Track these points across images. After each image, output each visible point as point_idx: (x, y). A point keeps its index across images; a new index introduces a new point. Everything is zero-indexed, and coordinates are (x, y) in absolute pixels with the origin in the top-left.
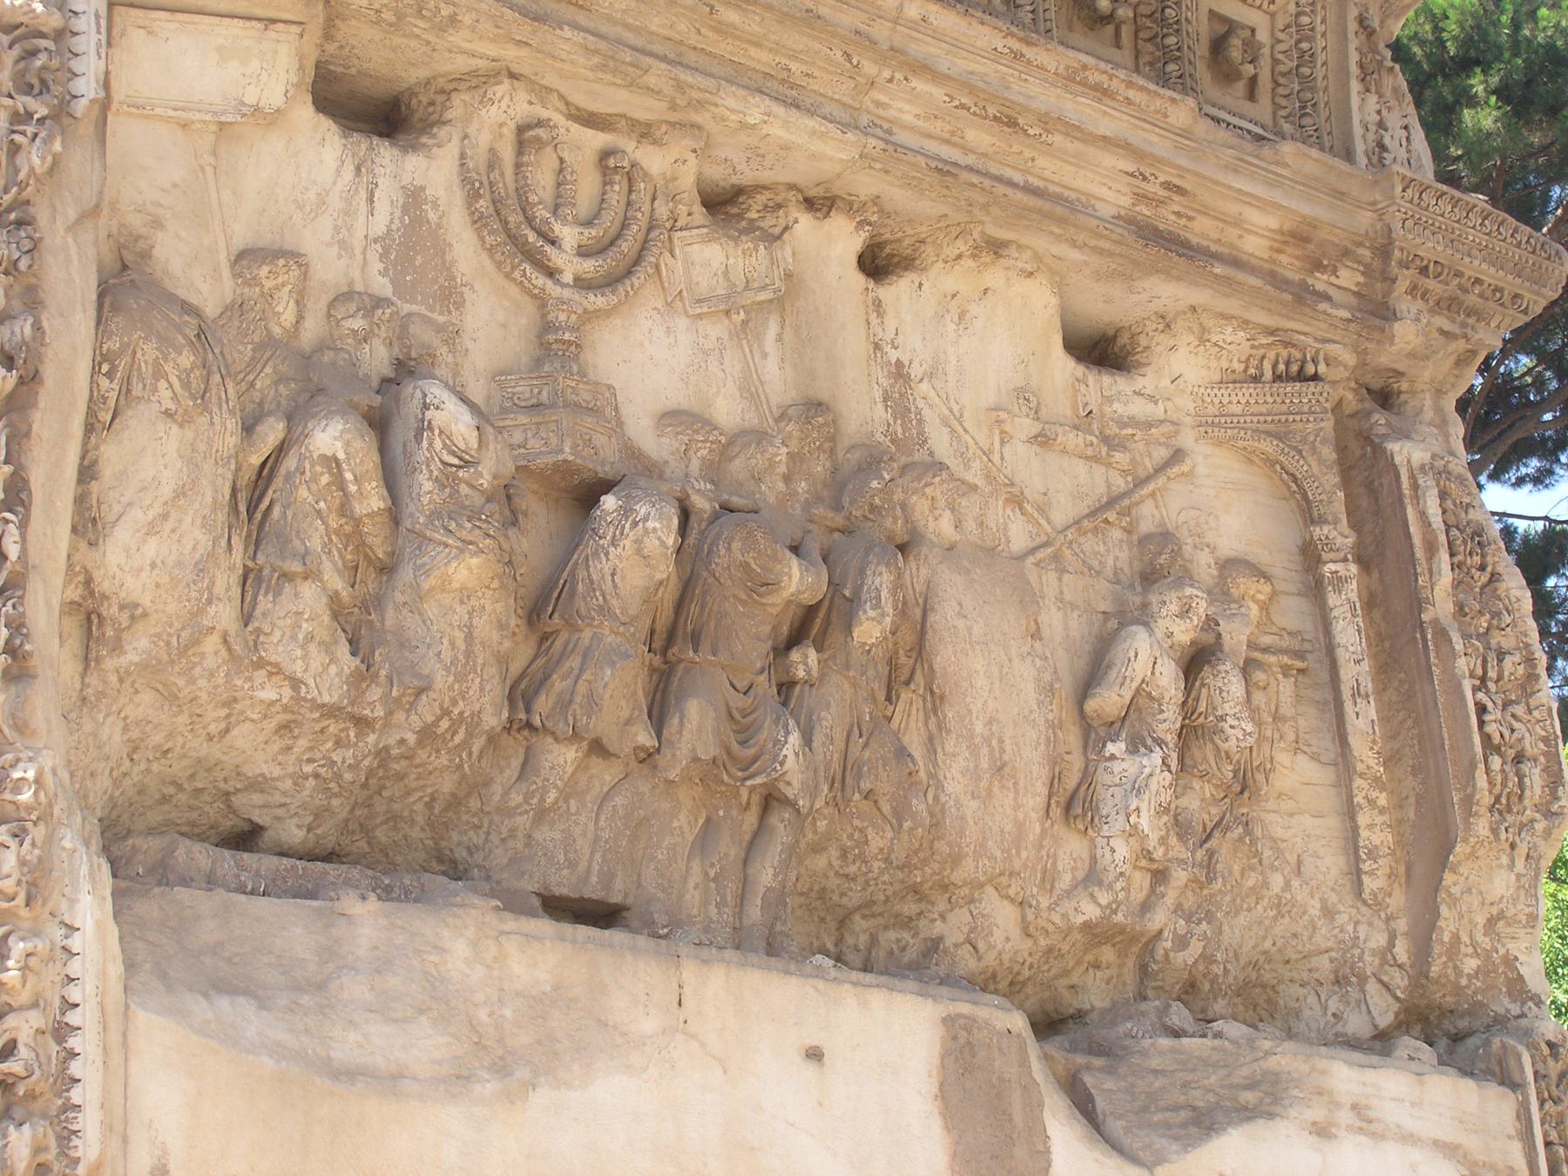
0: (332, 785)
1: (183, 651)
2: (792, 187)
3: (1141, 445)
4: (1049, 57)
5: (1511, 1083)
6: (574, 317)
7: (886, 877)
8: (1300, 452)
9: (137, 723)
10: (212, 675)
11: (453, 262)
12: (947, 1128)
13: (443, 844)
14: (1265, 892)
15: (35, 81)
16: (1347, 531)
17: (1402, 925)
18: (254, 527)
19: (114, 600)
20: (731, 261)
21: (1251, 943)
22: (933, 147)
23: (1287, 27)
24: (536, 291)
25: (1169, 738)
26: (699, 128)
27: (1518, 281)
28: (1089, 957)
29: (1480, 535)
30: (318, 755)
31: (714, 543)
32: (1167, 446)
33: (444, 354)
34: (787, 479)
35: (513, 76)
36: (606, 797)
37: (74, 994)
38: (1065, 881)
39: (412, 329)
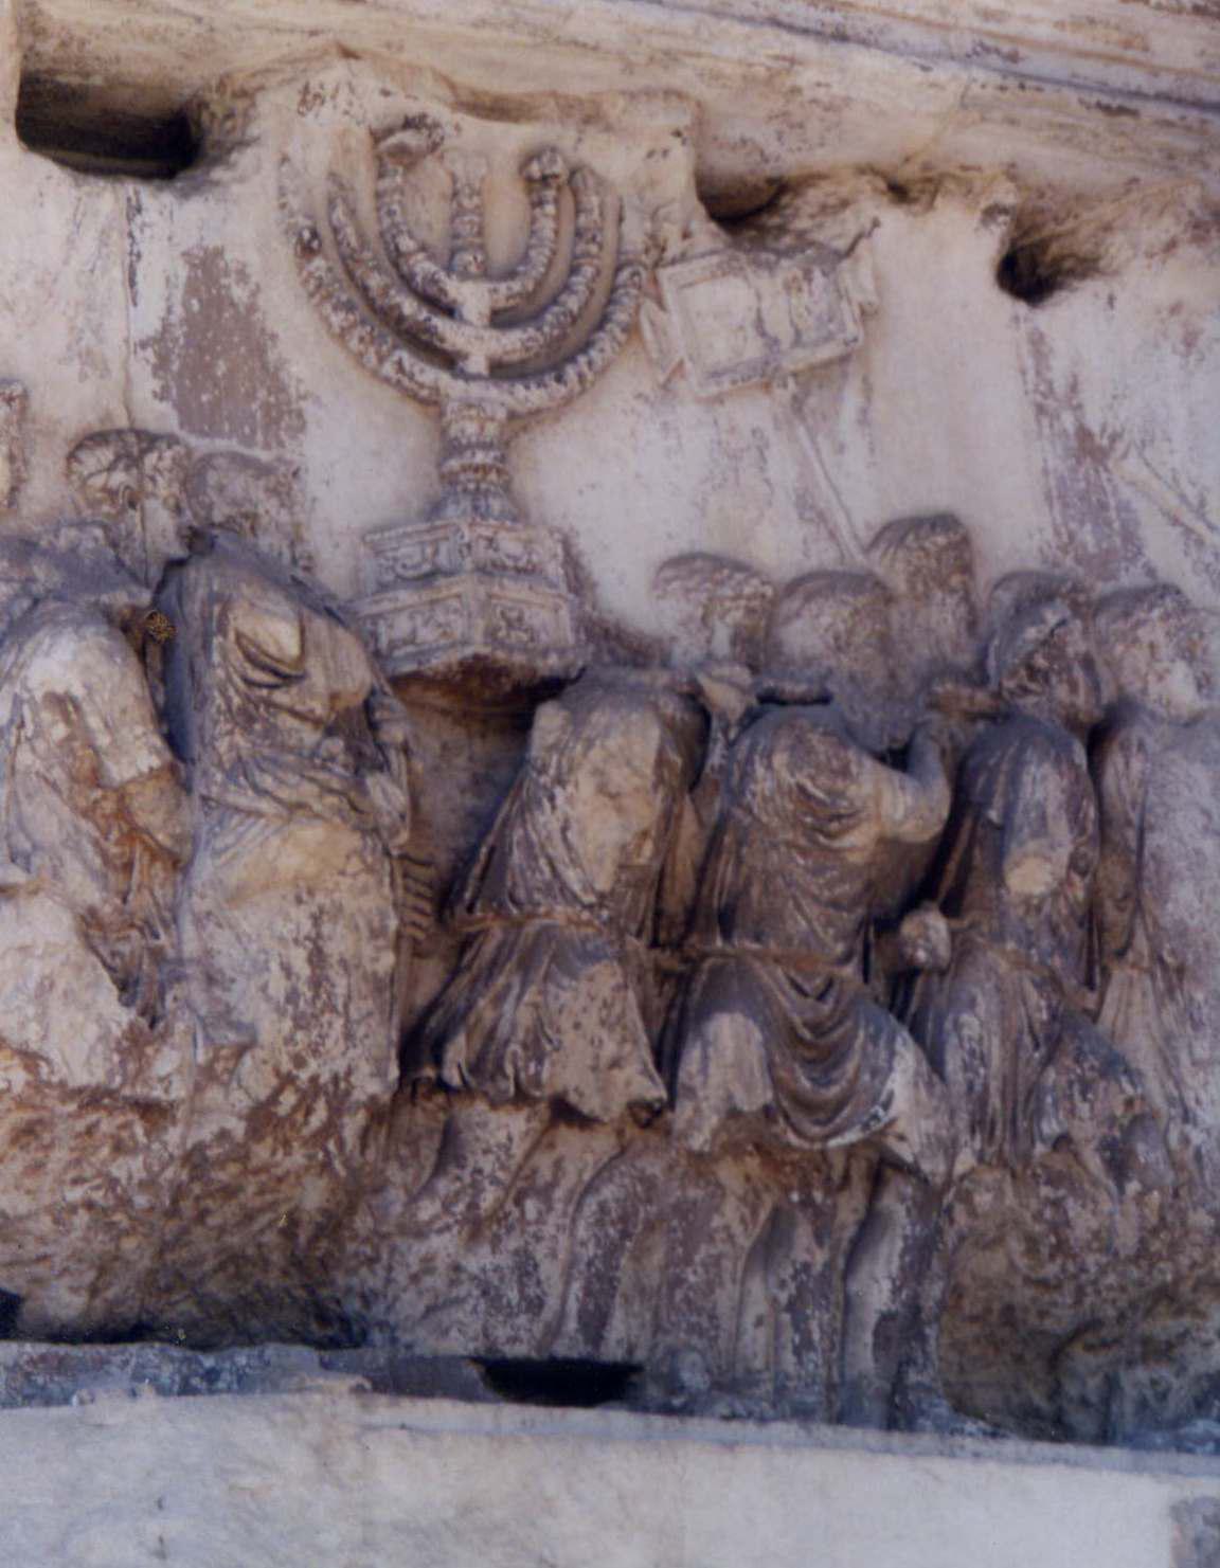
0: (118, 1217)
2: (863, 170)
7: (1111, 1279)
11: (282, 363)
13: (324, 1293)
24: (424, 393)
26: (680, 95)
30: (88, 1172)
31: (749, 761)
33: (273, 512)
35: (348, 54)
36: (590, 1188)
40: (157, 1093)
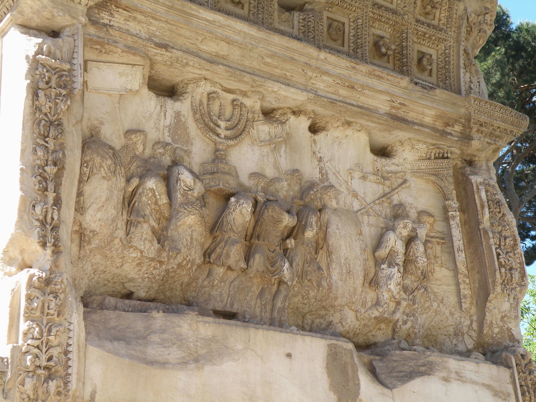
1: (109, 244)
2: (289, 108)
3: (394, 179)
4: (364, 68)
5: (509, 367)
6: (224, 147)
7: (315, 304)
8: (442, 180)
9: (96, 264)
10: (117, 250)
12: (328, 377)
13: (186, 296)
14: (431, 308)
15: (62, 84)
16: (456, 202)
17: (475, 318)
18: (130, 208)
19: (88, 230)
20: (271, 130)
21: (428, 323)
22: (330, 95)
23: (442, 54)
25: (400, 263)
26: (260, 92)
27: (512, 127)
28: (378, 327)
29: (499, 203)
30: (149, 272)
31: (264, 210)
32: (402, 178)
34: (287, 191)
35: (205, 79)
36: (232, 282)
37: (70, 342)
38: (369, 304)
39: (177, 152)
40: (162, 259)
